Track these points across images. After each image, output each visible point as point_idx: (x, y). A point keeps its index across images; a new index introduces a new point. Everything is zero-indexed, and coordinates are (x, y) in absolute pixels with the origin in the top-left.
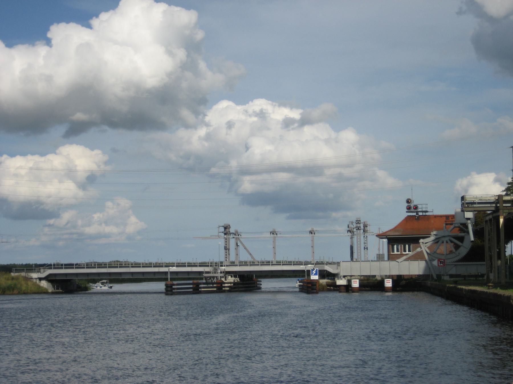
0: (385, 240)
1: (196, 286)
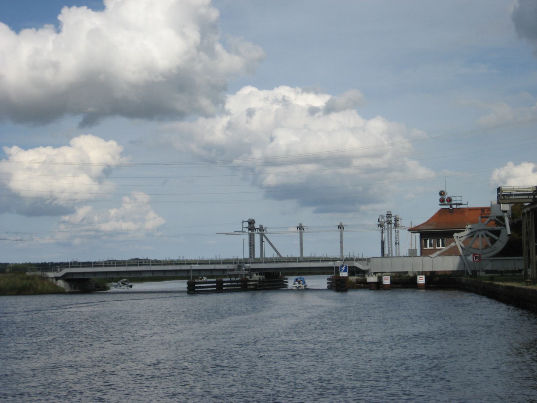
0: (418, 235)
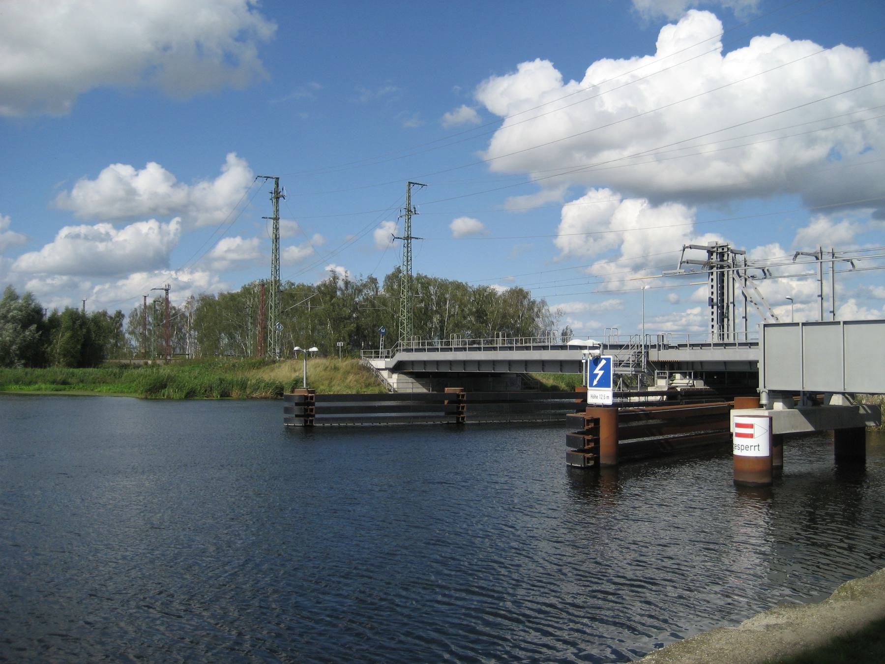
1: (448, 403)
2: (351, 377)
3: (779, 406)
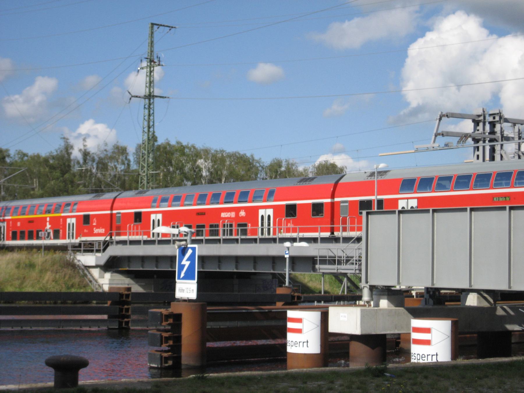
1: (111, 305)
2: (48, 276)
3: (384, 303)
